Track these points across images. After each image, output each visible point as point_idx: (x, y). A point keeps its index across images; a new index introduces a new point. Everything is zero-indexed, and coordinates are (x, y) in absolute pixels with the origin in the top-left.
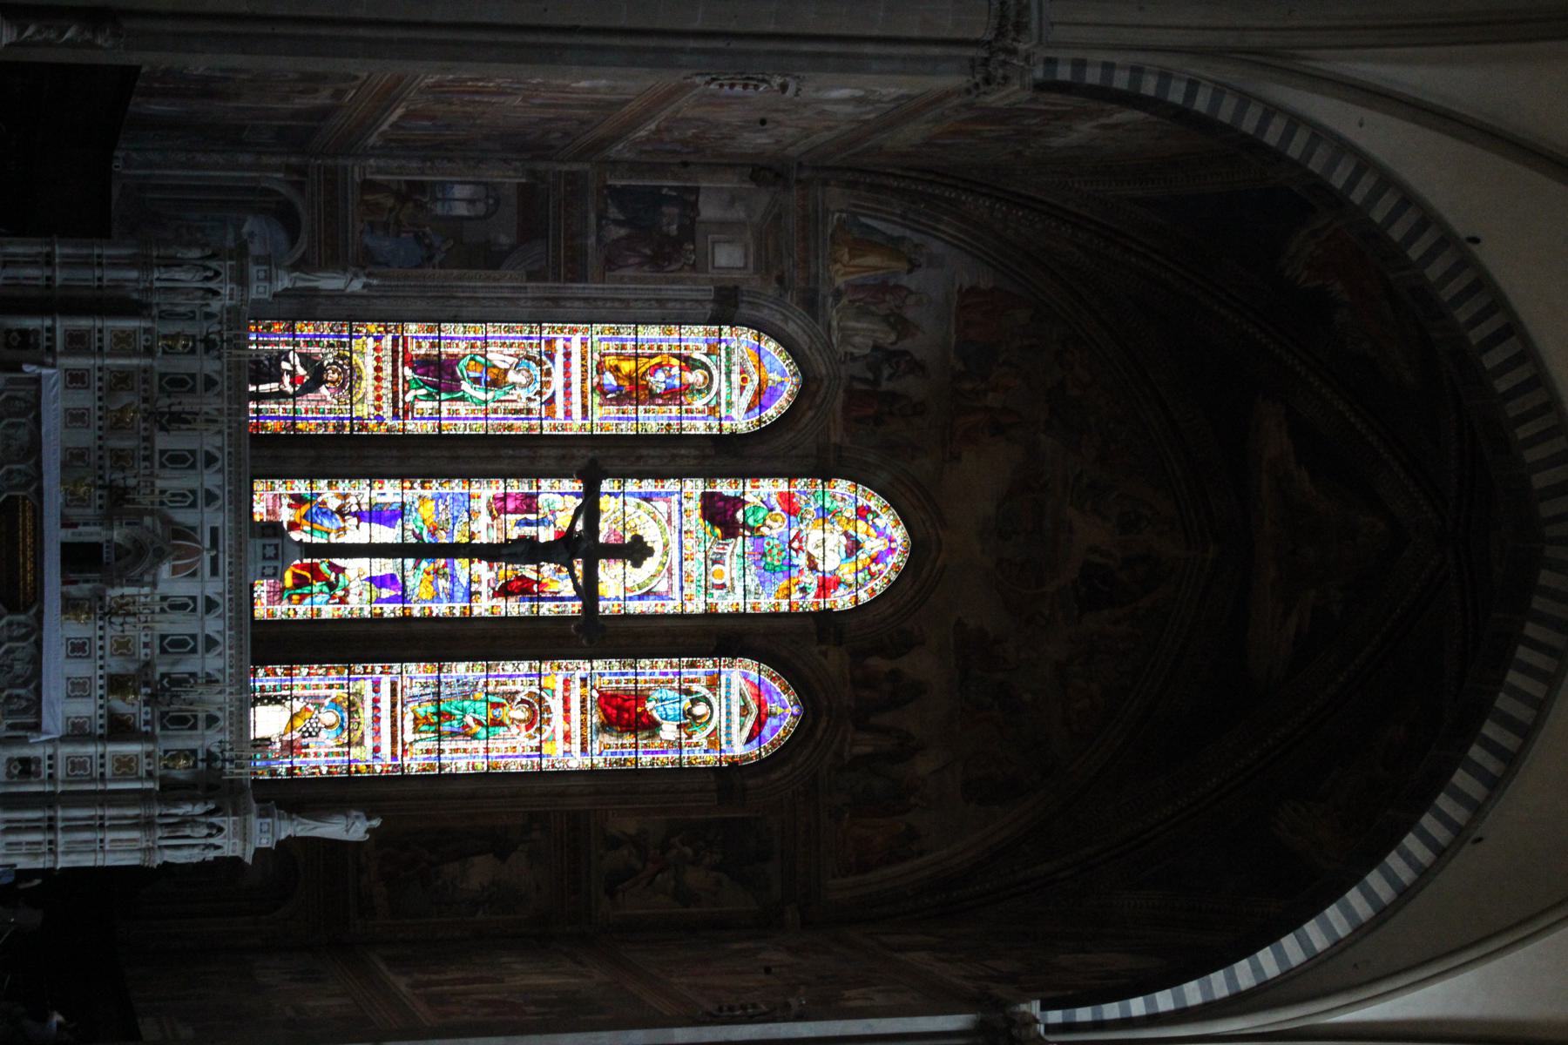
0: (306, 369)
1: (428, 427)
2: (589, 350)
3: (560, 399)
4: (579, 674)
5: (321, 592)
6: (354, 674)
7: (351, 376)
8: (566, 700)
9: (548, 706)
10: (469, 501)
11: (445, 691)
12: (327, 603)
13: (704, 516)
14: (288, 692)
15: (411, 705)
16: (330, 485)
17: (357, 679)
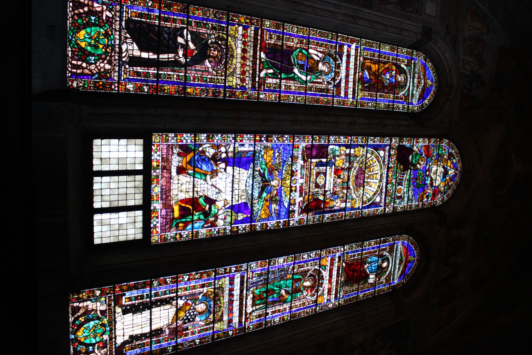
0: (195, 45)
1: (273, 97)
2: (359, 54)
3: (343, 85)
4: (338, 255)
5: (199, 219)
6: (219, 274)
7: (226, 54)
8: (331, 271)
9: (323, 276)
10: (293, 150)
11: (271, 276)
12: (203, 227)
13: (397, 159)
14: (175, 294)
15: (252, 289)
16: (208, 138)
17: (220, 278)
